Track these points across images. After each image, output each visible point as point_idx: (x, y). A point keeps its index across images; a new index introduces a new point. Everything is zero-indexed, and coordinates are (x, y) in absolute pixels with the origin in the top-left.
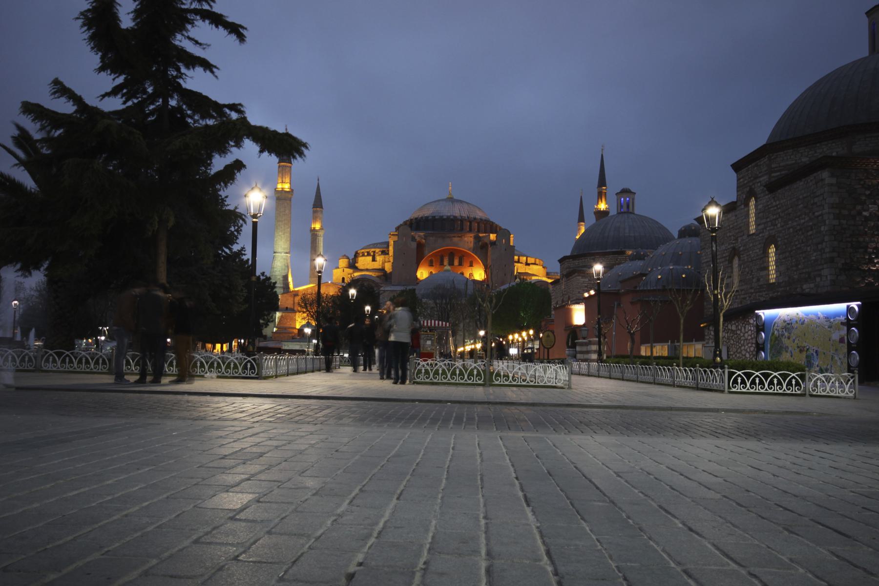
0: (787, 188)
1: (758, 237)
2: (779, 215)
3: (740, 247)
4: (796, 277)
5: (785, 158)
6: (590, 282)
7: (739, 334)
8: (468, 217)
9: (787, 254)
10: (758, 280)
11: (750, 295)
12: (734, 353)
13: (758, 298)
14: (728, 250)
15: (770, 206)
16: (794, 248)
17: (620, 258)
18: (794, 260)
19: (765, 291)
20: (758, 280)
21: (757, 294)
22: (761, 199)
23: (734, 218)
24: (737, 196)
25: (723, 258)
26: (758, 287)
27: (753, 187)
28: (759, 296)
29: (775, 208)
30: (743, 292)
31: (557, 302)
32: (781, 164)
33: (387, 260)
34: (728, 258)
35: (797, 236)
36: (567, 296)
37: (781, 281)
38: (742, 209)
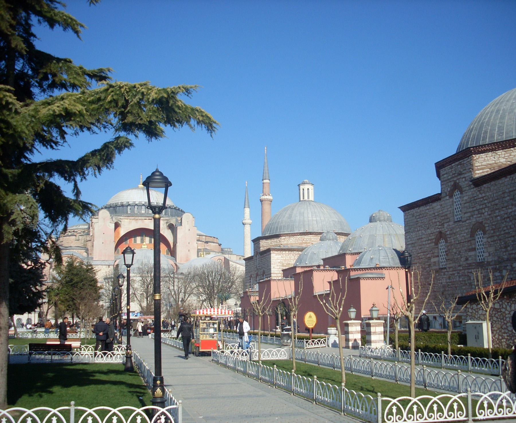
0: (493, 183)
1: (465, 223)
2: (486, 206)
3: (446, 231)
4: (506, 257)
5: (486, 159)
6: (282, 259)
7: (504, 312)
8: (157, 203)
9: (496, 238)
10: (467, 259)
11: (459, 271)
12: (499, 329)
13: (466, 274)
14: (434, 234)
15: (475, 198)
16: (503, 233)
17: (306, 238)
18: (503, 243)
19: (474, 268)
20: (467, 259)
21: (466, 271)
22: (466, 191)
23: (439, 207)
24: (441, 189)
25: (429, 240)
26: (467, 265)
27: (458, 181)
28: (468, 272)
29: (482, 199)
30: (451, 269)
31: (251, 275)
32: (483, 163)
33: (88, 239)
34: (434, 240)
35: (504, 223)
36: (262, 270)
37: (491, 260)
38: (446, 200)
